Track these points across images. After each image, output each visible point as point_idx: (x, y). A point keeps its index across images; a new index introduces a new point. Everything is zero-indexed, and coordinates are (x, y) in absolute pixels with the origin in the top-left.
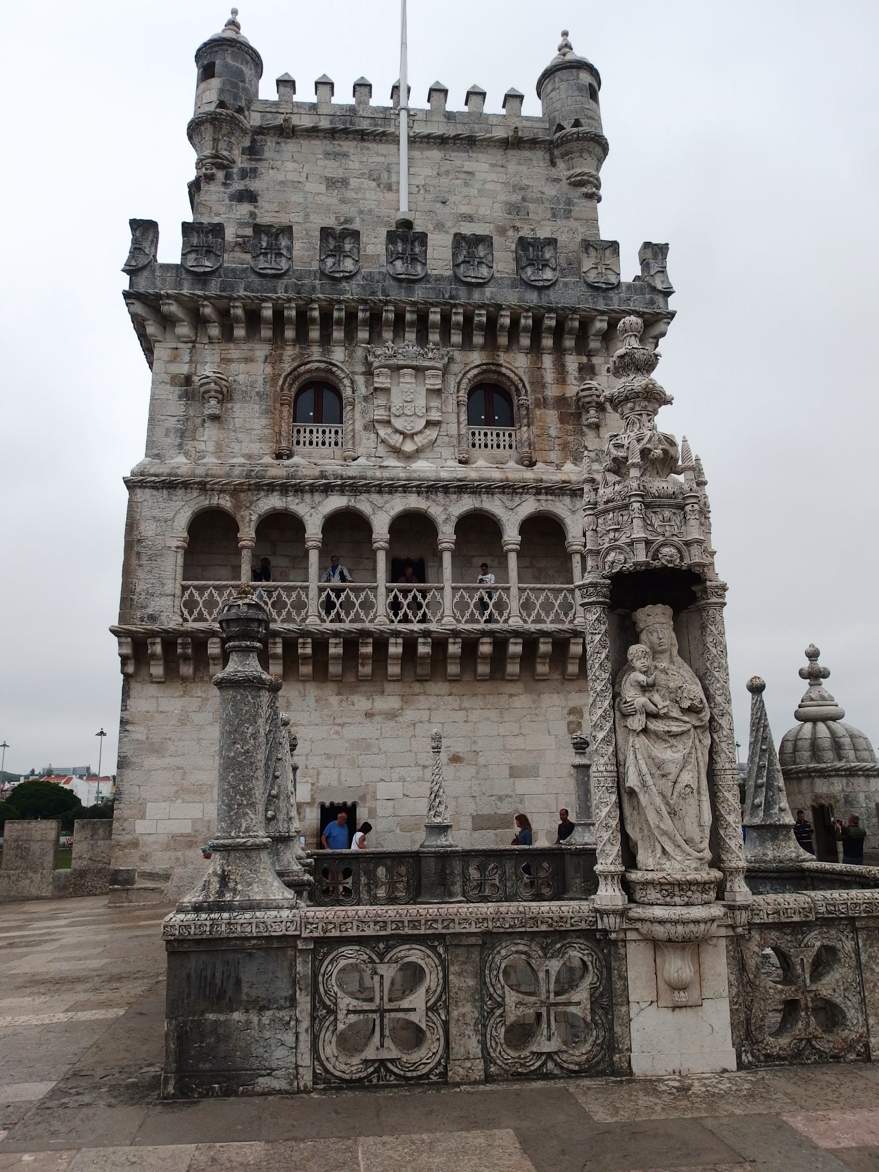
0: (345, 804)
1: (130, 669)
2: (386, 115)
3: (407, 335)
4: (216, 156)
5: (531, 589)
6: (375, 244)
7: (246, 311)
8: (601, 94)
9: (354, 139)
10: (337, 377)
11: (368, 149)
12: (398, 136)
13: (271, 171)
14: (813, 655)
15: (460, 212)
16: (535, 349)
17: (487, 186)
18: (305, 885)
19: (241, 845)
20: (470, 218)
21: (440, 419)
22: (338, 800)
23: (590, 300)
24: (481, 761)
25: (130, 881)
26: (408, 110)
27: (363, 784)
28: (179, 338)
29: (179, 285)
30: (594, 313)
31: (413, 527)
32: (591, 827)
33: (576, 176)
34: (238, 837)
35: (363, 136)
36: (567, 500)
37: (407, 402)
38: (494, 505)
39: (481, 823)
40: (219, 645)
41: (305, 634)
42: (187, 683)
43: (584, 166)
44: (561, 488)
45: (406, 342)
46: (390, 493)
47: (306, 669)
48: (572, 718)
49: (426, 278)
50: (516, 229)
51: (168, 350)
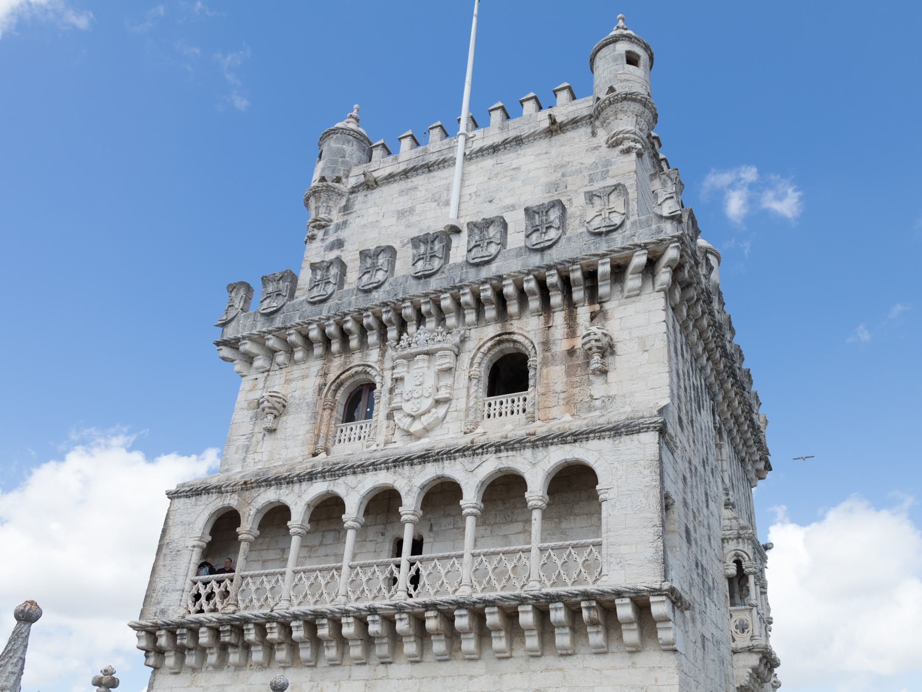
13: (358, 219)
15: (504, 204)
17: (531, 175)
21: (448, 395)
23: (592, 247)
30: (596, 259)
31: (384, 503)
36: (528, 453)
40: (206, 634)
41: (271, 619)
44: (520, 442)
46: (364, 472)
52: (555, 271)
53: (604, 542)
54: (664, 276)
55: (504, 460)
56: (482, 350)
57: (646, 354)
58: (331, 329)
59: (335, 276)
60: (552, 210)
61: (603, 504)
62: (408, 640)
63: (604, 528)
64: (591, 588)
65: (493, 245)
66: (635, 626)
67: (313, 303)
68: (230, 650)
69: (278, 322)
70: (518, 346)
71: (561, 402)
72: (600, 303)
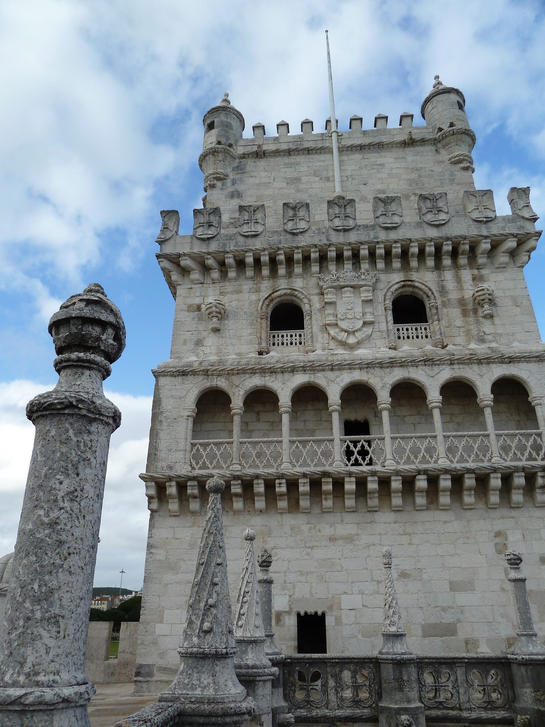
0: (316, 613)
1: (155, 506)
3: (346, 266)
6: (320, 214)
7: (235, 260)
8: (466, 108)
9: (303, 154)
10: (299, 298)
12: (332, 148)
15: (377, 188)
16: (438, 266)
17: (394, 171)
18: (244, 714)
19: (13, 703)
21: (373, 320)
22: (311, 610)
24: (425, 576)
25: (150, 674)
26: (338, 133)
27: (330, 596)
28: (192, 281)
32: (534, 638)
34: (15, 684)
35: (309, 151)
36: (475, 367)
37: (348, 309)
39: (431, 631)
41: (281, 476)
42: (196, 516)
44: (469, 359)
45: (345, 270)
47: (283, 504)
48: (498, 540)
49: (356, 227)
51: (186, 290)
52: (450, 242)
57: (518, 308)
58: (265, 258)
60: (440, 200)
61: (536, 407)
62: (396, 495)
67: (247, 237)
69: (214, 247)
70: (416, 290)
71: (462, 334)
72: (477, 269)
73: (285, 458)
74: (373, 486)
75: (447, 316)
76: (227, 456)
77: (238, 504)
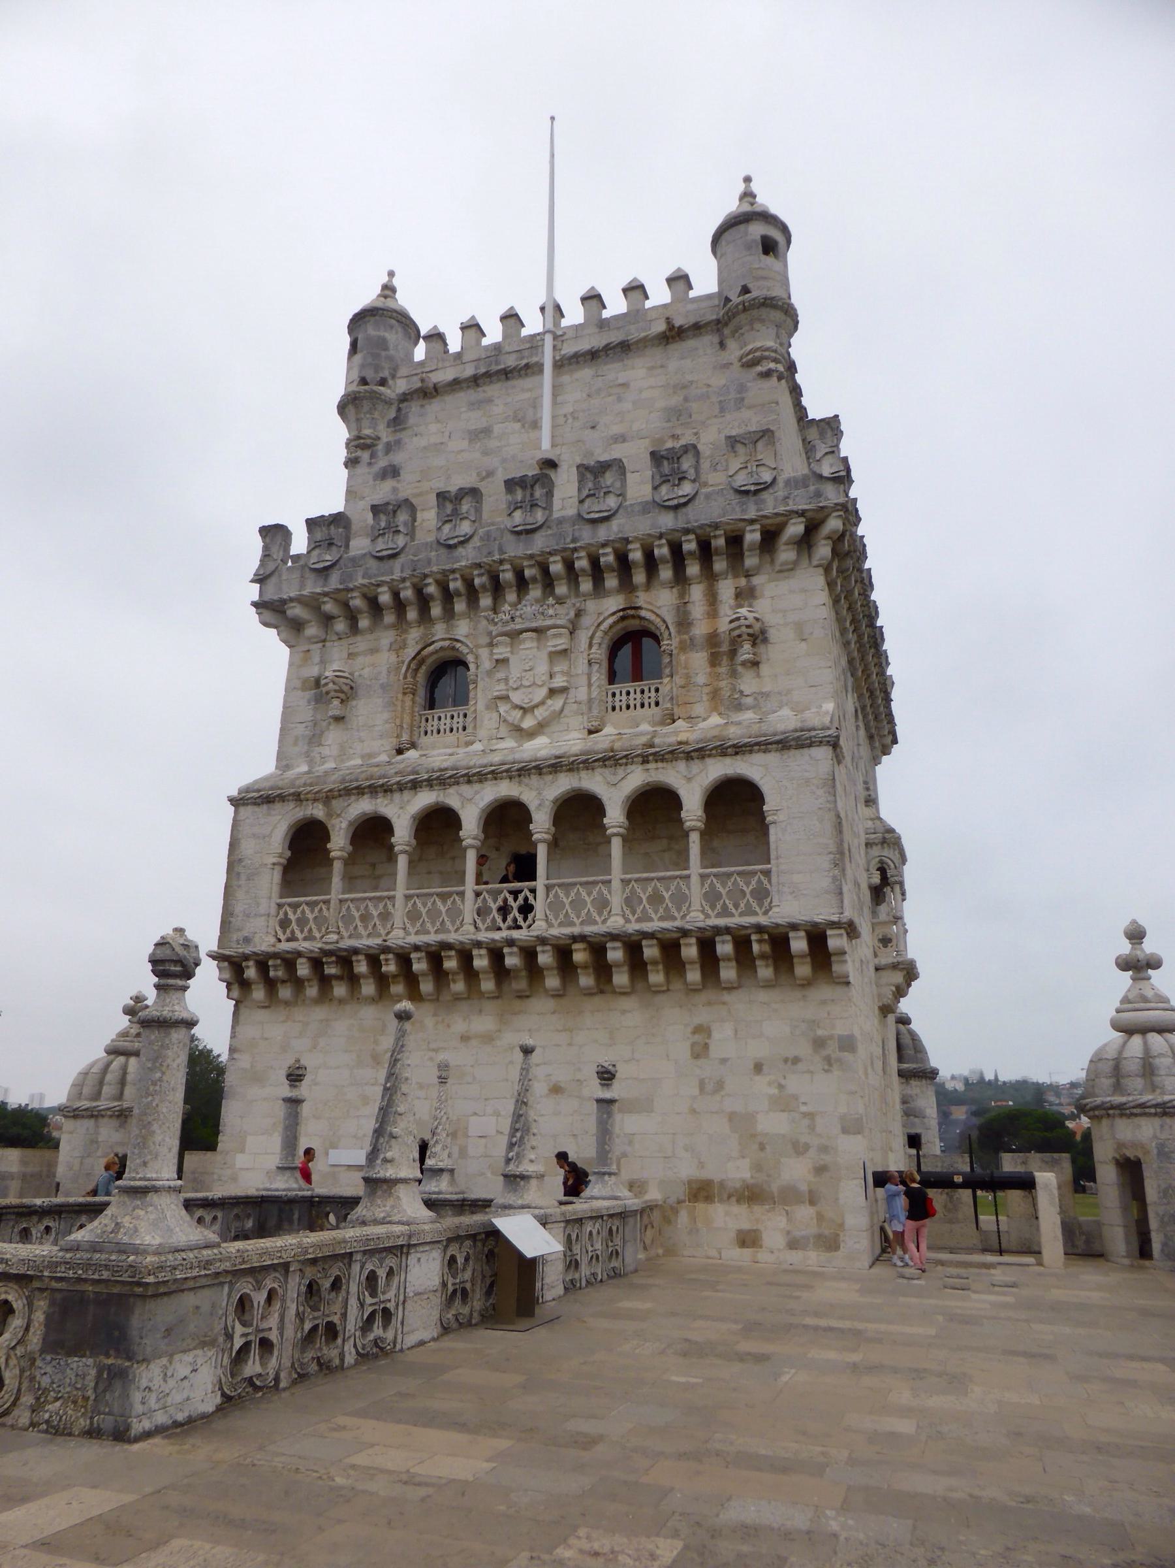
1: (236, 993)
2: (535, 341)
4: (359, 438)
5: (636, 880)
9: (499, 380)
11: (514, 387)
13: (415, 439)
14: (1136, 935)
20: (621, 438)
21: (565, 684)
23: (738, 509)
29: (302, 586)
30: (742, 524)
31: (507, 818)
32: (606, 1178)
33: (748, 354)
35: (507, 374)
36: (682, 765)
38: (594, 783)
41: (386, 950)
43: (763, 339)
44: (672, 752)
46: (481, 782)
48: (696, 1036)
50: (675, 437)
52: (692, 537)
53: (774, 869)
54: (823, 550)
55: (653, 773)
56: (602, 627)
57: (803, 644)
58: (407, 593)
59: (405, 524)
63: (773, 855)
64: (763, 920)
65: (611, 496)
66: (808, 959)
67: (380, 559)
68: (334, 983)
69: (334, 581)
70: (646, 623)
71: (705, 698)
73: (398, 922)
74: (512, 960)
75: (686, 668)
76: (320, 921)
77: (340, 990)
